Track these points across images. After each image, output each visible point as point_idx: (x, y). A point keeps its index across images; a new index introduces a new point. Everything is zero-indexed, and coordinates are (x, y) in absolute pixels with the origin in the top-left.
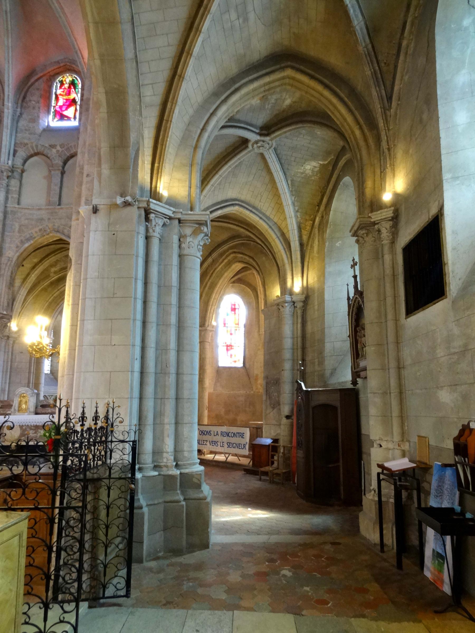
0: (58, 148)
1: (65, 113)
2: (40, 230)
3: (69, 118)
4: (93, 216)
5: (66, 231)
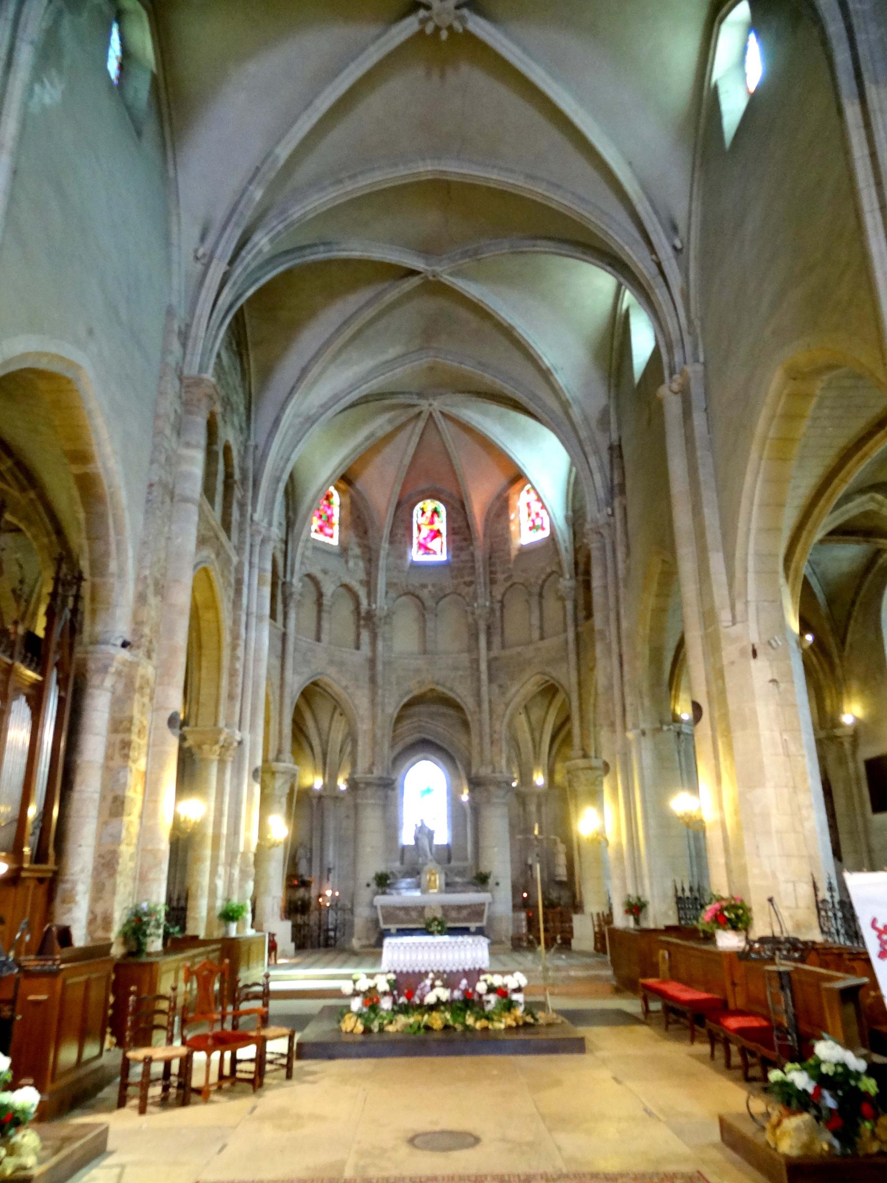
0: (430, 588)
1: (430, 545)
2: (419, 682)
3: (435, 553)
4: (642, 738)
5: (448, 684)
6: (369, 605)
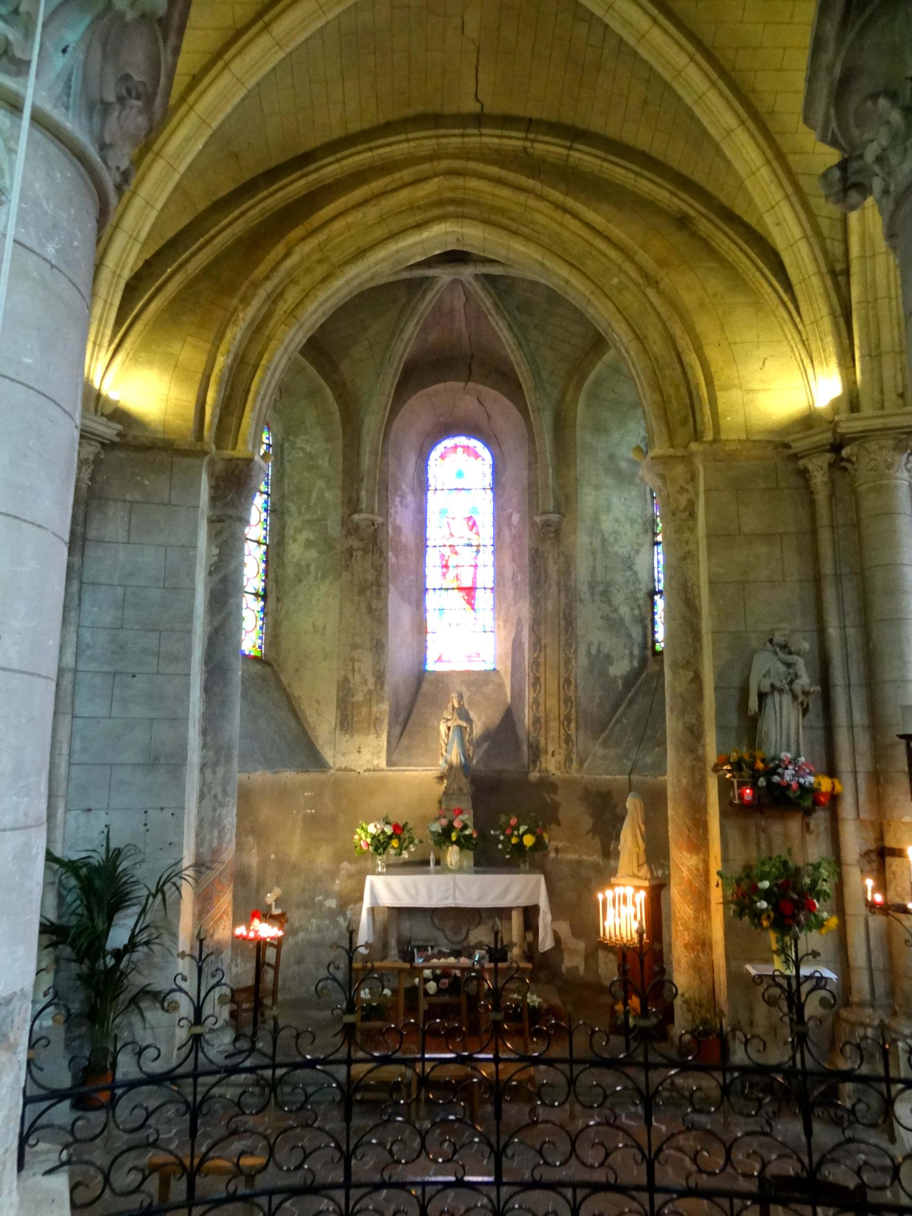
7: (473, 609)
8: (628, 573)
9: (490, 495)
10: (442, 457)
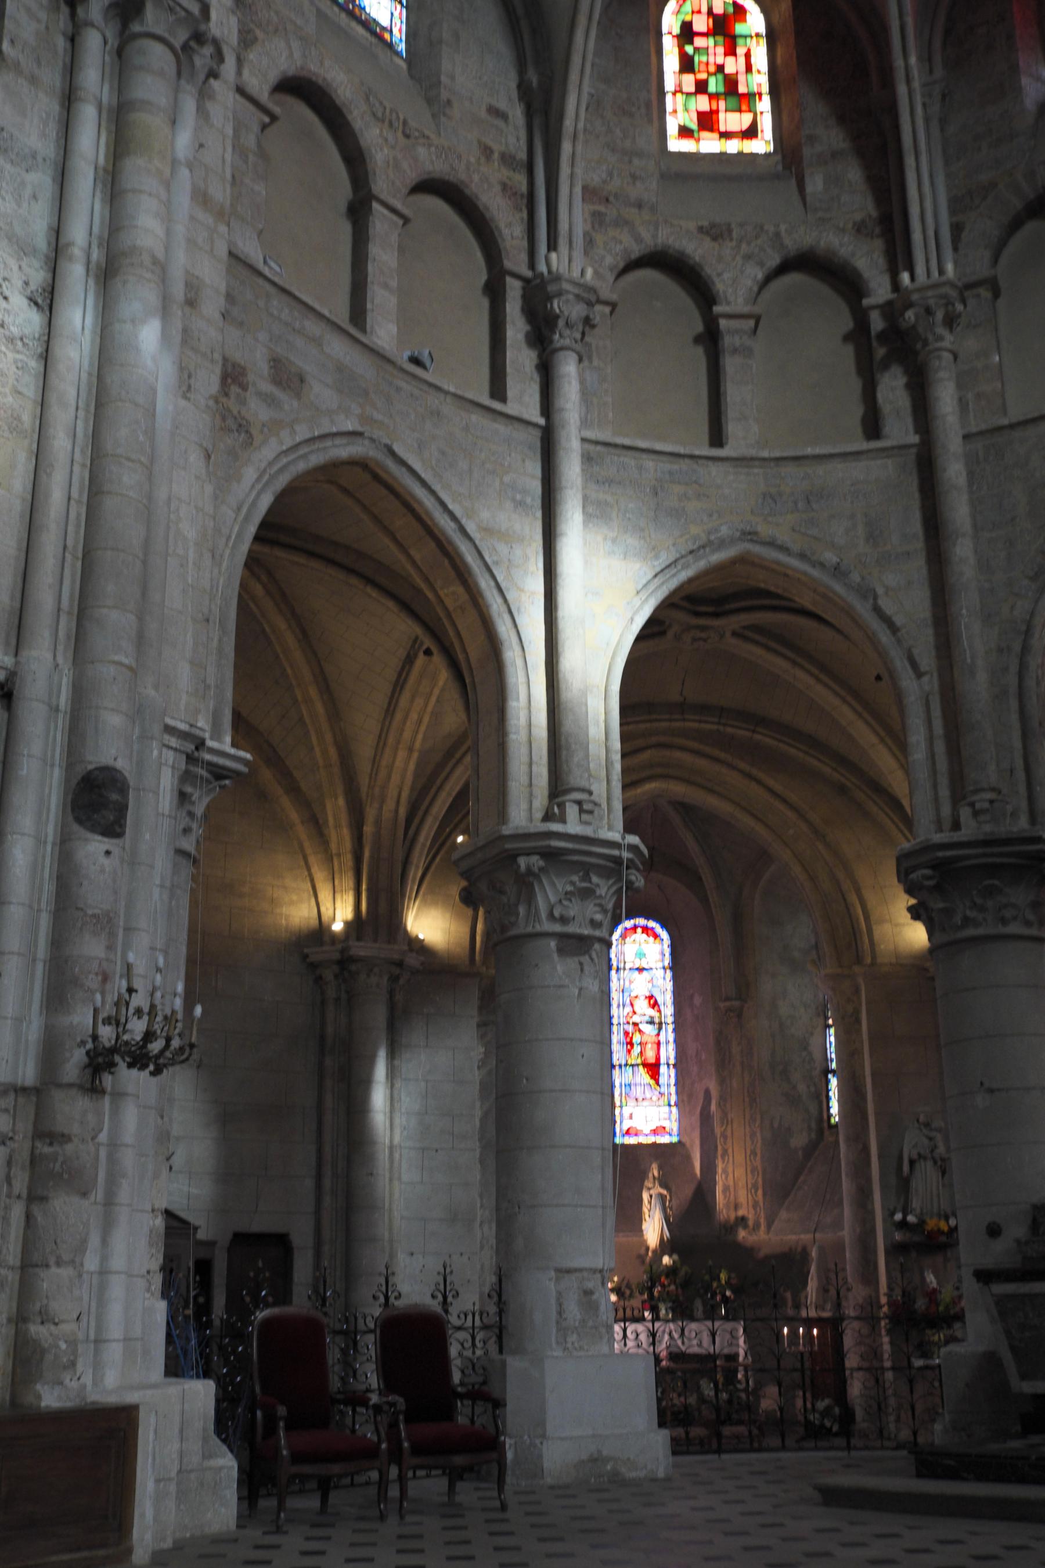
6: (896, 286)
7: (657, 1083)
8: (804, 1054)
9: (669, 974)
10: (624, 936)
